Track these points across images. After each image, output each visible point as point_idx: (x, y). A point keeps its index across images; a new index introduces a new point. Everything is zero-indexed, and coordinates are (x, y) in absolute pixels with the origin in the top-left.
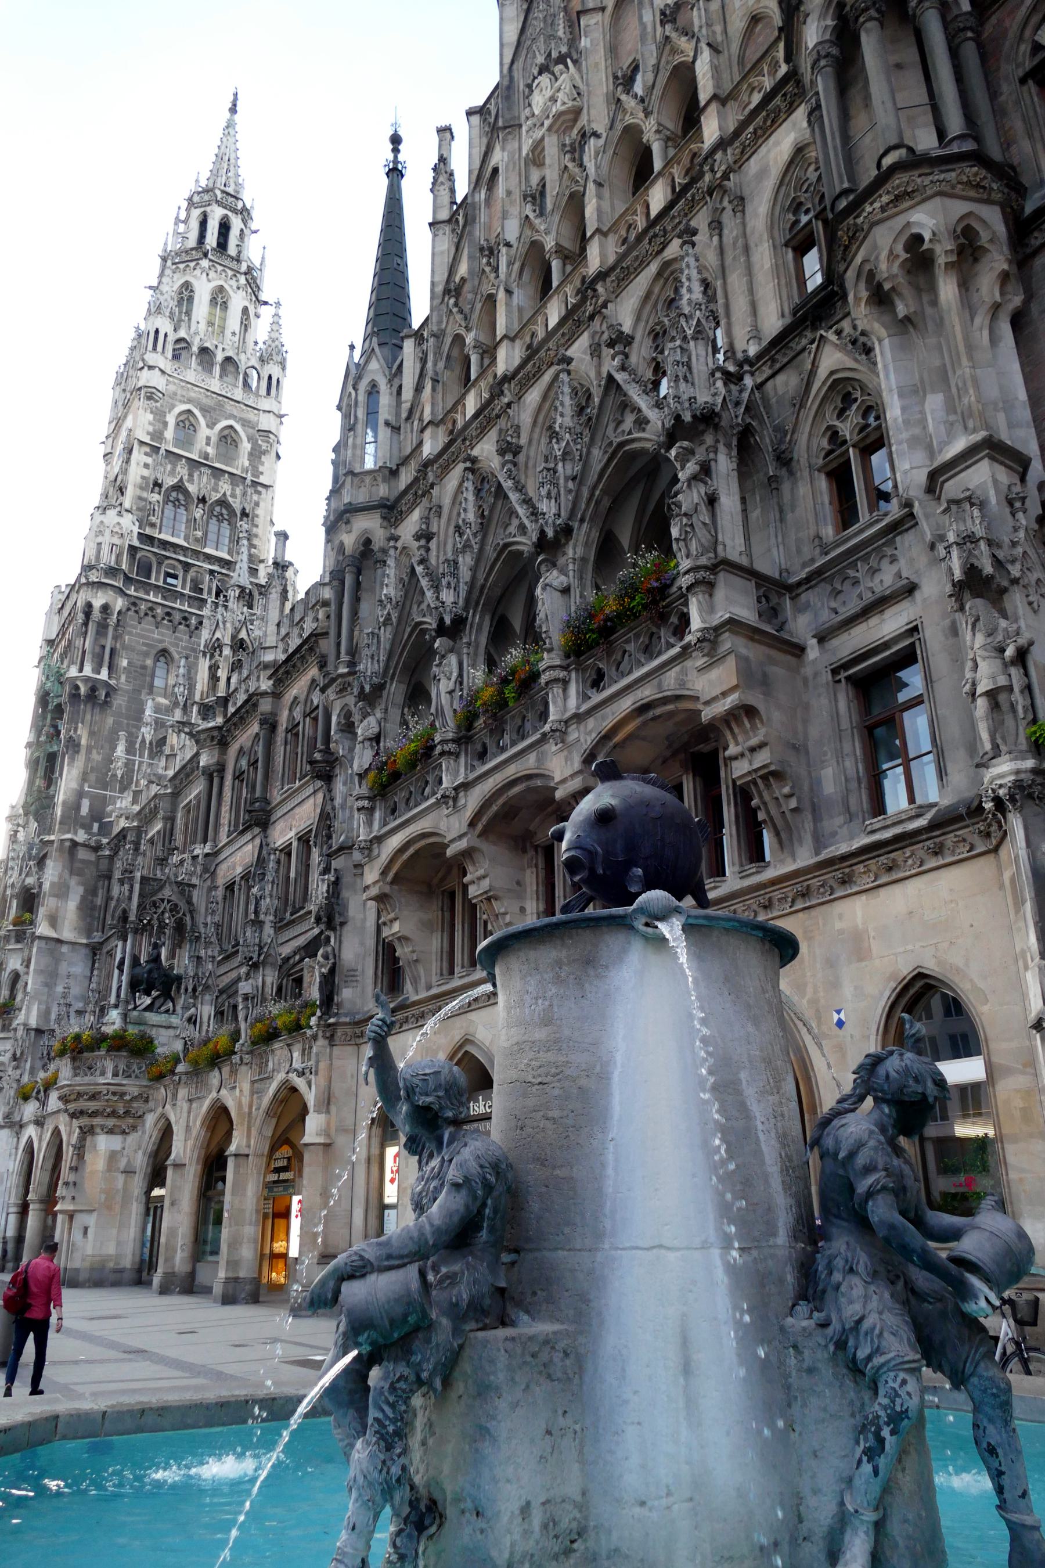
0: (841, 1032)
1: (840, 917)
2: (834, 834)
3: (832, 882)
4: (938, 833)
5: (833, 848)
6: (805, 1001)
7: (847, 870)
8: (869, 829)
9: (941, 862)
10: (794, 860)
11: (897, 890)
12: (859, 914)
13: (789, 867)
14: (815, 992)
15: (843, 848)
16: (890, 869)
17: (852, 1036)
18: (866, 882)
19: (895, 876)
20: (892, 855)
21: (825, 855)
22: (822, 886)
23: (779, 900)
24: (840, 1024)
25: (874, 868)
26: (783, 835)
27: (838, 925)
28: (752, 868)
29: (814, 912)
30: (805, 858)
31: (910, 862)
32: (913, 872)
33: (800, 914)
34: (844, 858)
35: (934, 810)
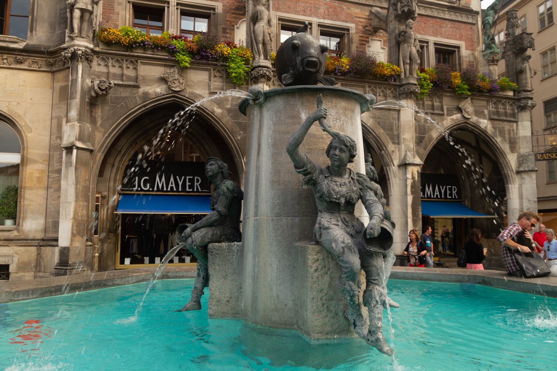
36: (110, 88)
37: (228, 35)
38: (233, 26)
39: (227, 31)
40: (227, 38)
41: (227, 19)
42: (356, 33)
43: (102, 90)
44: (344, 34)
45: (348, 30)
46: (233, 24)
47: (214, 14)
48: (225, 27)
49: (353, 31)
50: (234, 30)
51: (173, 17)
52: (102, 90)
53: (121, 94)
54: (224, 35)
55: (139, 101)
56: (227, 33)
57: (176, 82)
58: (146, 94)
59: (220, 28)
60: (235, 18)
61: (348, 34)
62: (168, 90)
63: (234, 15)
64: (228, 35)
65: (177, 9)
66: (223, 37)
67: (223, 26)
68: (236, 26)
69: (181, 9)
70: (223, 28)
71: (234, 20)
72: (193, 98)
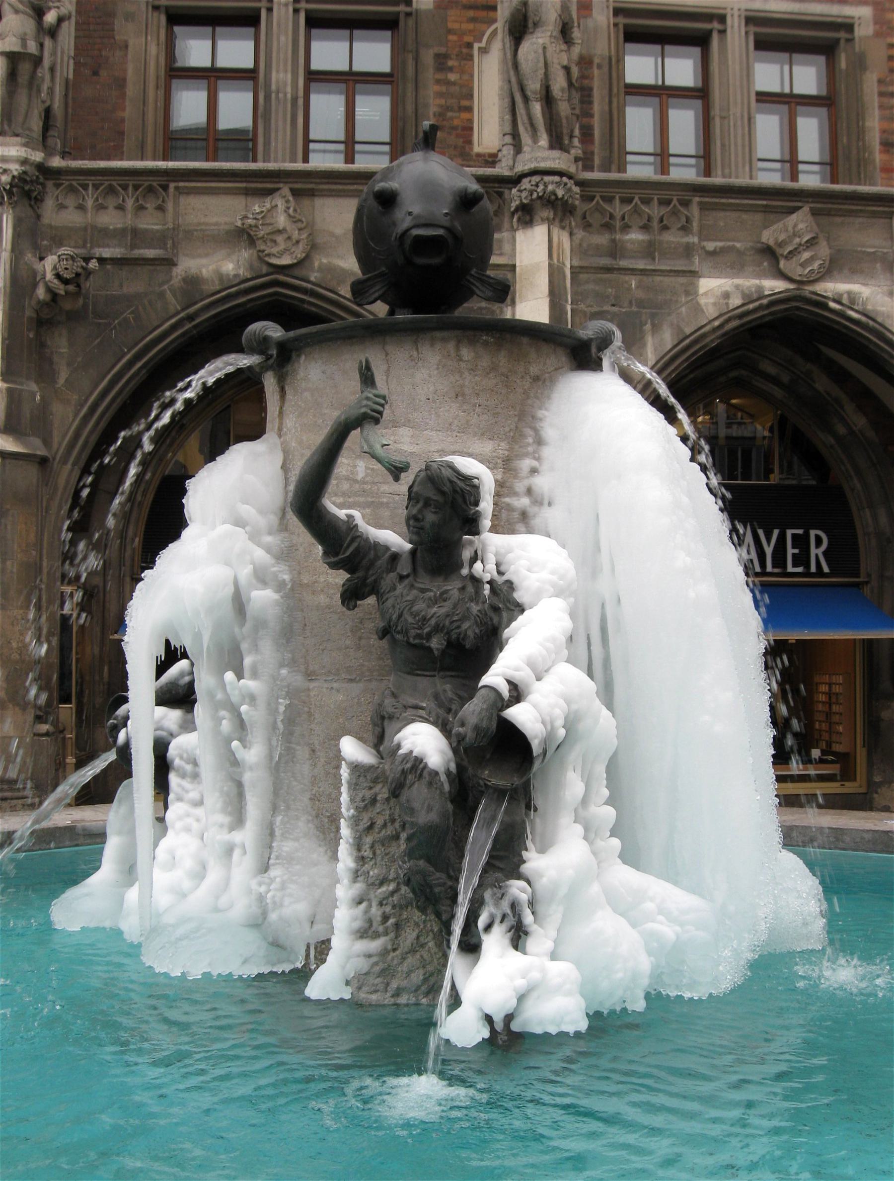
36: (89, 273)
37: (452, 77)
38: (470, 46)
39: (450, 63)
40: (448, 83)
41: (450, 25)
42: (878, 34)
43: (66, 282)
44: (837, 41)
45: (848, 27)
46: (467, 39)
47: (408, 14)
48: (443, 50)
49: (864, 31)
50: (470, 57)
51: (283, 38)
52: (66, 282)
53: (121, 286)
54: (439, 76)
55: (173, 304)
56: (451, 69)
57: (280, 239)
58: (192, 282)
59: (428, 57)
60: (473, 20)
61: (850, 41)
62: (256, 264)
63: (471, 13)
64: (452, 77)
65: (296, 11)
66: (438, 82)
67: (437, 50)
68: (476, 46)
69: (307, 12)
70: (437, 56)
71: (471, 26)
72: (333, 284)
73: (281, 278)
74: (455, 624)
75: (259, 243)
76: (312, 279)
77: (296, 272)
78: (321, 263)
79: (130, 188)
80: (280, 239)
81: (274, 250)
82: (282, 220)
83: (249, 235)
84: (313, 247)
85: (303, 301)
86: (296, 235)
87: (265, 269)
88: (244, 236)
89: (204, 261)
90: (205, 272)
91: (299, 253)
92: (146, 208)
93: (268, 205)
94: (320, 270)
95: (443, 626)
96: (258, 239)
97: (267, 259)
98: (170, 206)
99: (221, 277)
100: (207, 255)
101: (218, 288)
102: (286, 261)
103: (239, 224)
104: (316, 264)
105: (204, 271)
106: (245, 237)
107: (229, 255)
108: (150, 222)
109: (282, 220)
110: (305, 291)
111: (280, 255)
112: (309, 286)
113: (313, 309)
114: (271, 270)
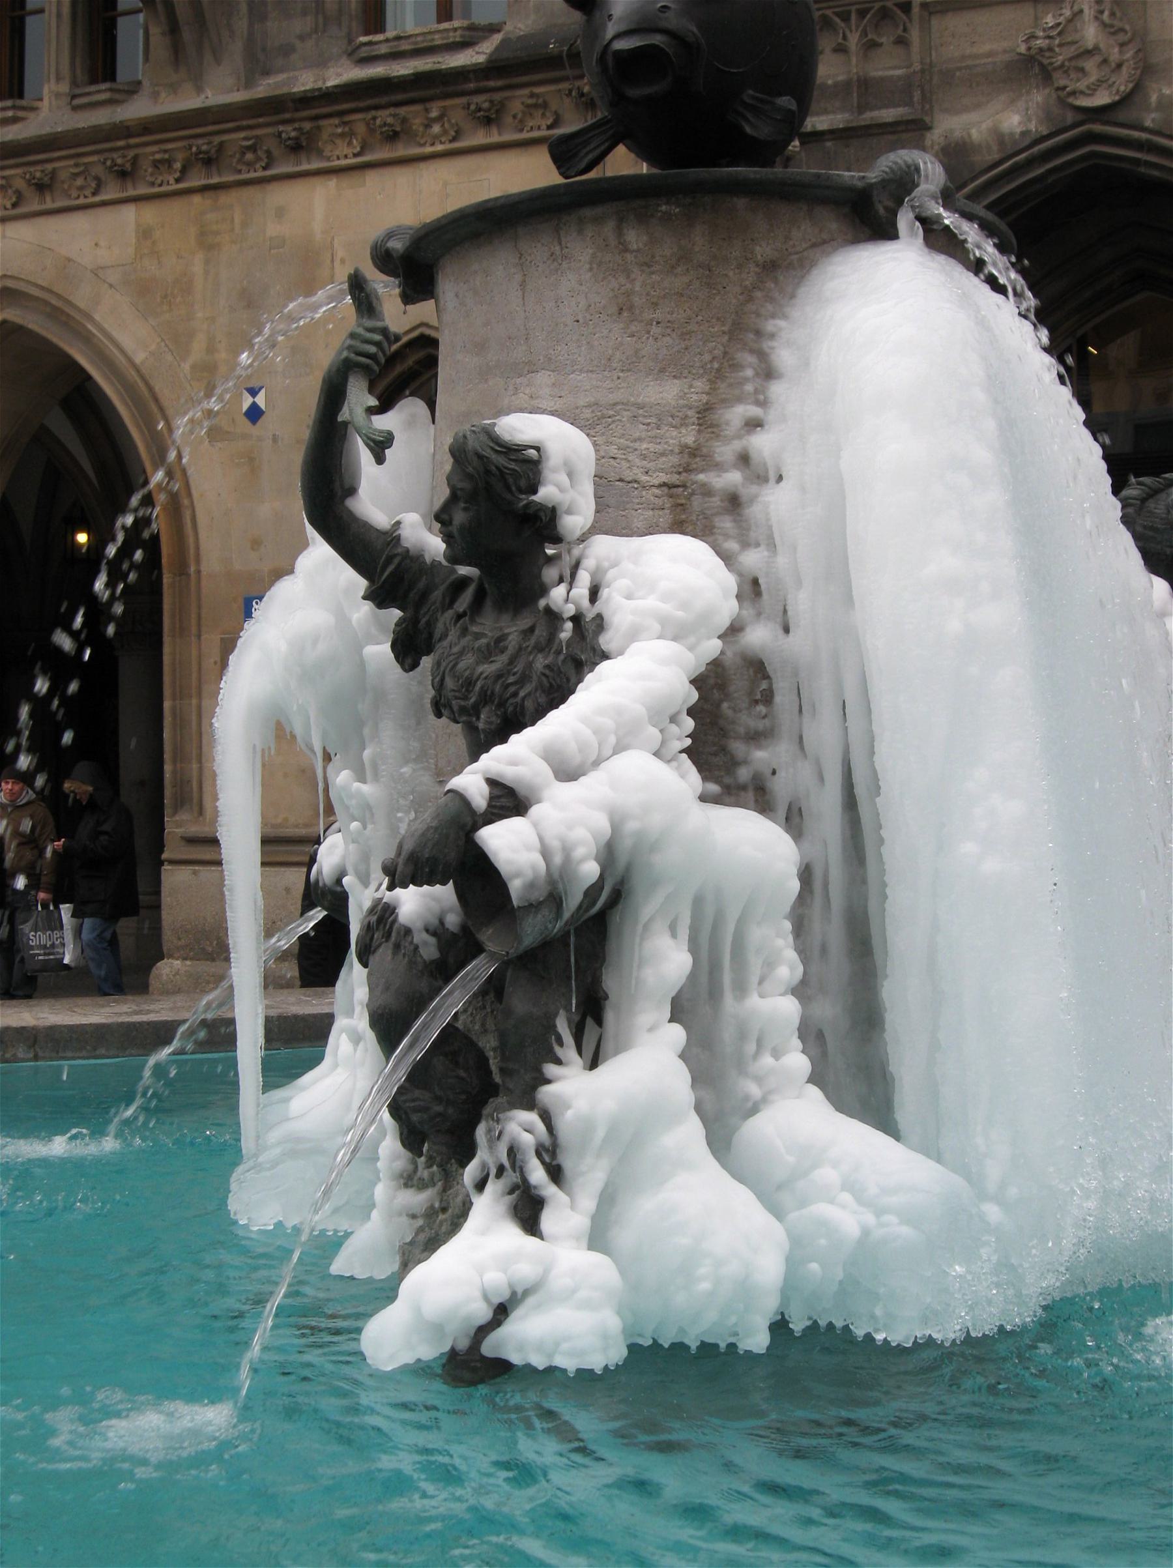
0: (255, 430)
1: (280, 213)
2: (287, 50)
3: (270, 144)
4: (500, 83)
5: (281, 77)
6: (186, 367)
7: (307, 126)
8: (364, 52)
9: (495, 138)
10: (199, 89)
11: (401, 178)
12: (319, 212)
13: (188, 102)
14: (211, 349)
15: (305, 81)
16: (393, 137)
17: (275, 439)
18: (343, 153)
19: (401, 151)
20: (402, 111)
21: (264, 88)
22: (253, 148)
23: (156, 164)
24: (254, 414)
25: (361, 129)
26: (187, 35)
27: (273, 229)
28: (101, 91)
29: (225, 198)
30: (220, 89)
31: (436, 129)
32: (439, 148)
33: (197, 199)
34: (305, 100)
35: (497, 38)
73: (1098, 128)
74: (512, 689)
75: (1056, 75)
76: (1148, 123)
77: (1122, 115)
78: (1161, 96)
79: (853, 17)
80: (1090, 65)
81: (1082, 85)
82: (1091, 33)
83: (1041, 64)
84: (1147, 70)
85: (1137, 162)
86: (1115, 55)
87: (1070, 117)
88: (1032, 68)
89: (973, 116)
90: (975, 135)
91: (1123, 83)
92: (881, 45)
93: (1067, 13)
94: (1160, 106)
95: (492, 693)
96: (1055, 69)
97: (1071, 100)
98: (915, 35)
99: (1000, 138)
100: (977, 106)
101: (996, 156)
102: (1102, 99)
103: (1022, 49)
104: (1154, 98)
105: (974, 133)
106: (1037, 69)
107: (1013, 101)
108: (887, 66)
109: (1091, 33)
110: (1139, 145)
111: (1092, 90)
112: (1144, 136)
113: (1156, 173)
114: (1080, 117)
